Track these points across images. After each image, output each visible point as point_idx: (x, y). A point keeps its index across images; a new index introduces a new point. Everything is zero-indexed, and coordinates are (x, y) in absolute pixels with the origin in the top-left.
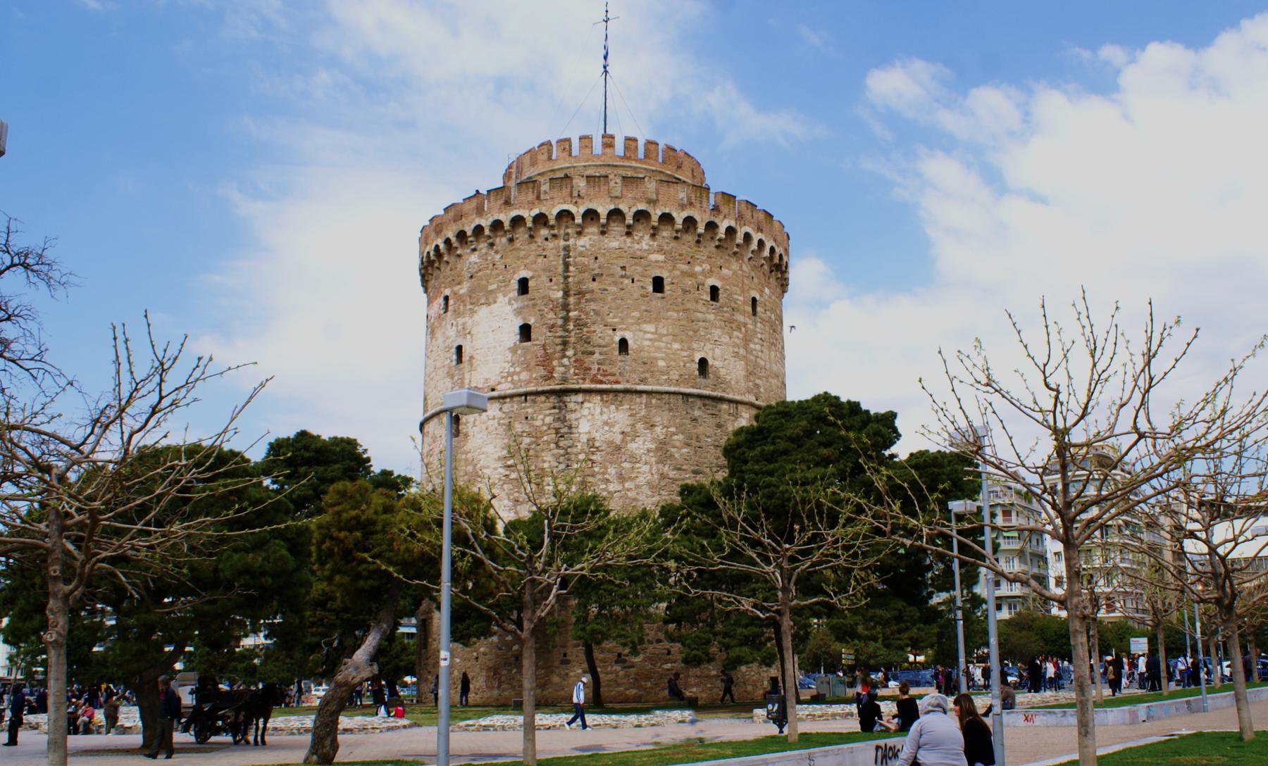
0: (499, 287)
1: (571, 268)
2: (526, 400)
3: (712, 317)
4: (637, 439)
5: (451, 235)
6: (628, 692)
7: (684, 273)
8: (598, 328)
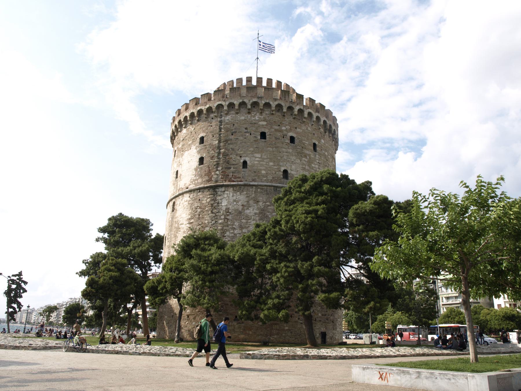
0: (193, 142)
1: (223, 130)
3: (291, 151)
4: (250, 208)
6: (239, 336)
7: (276, 130)
8: (233, 156)
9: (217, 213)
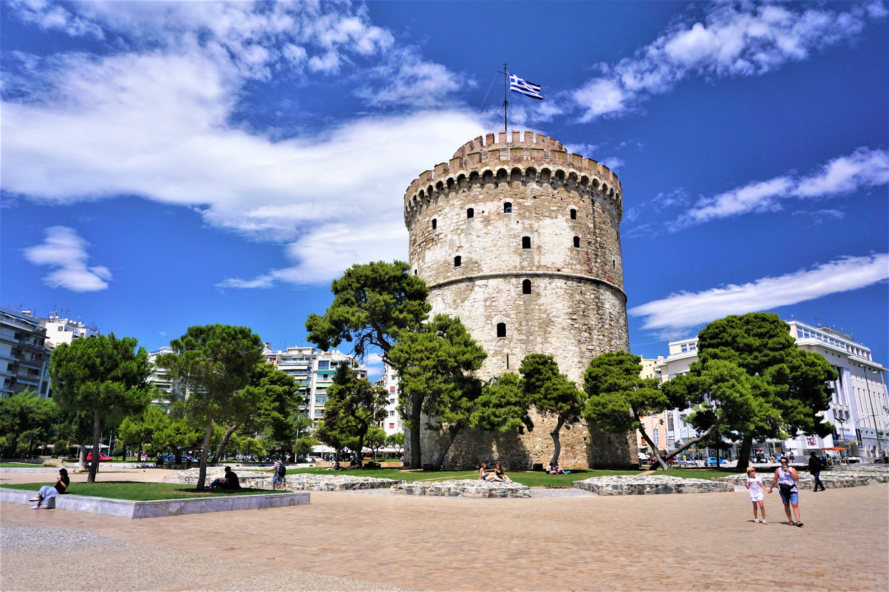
0: (558, 210)
5: (520, 166)
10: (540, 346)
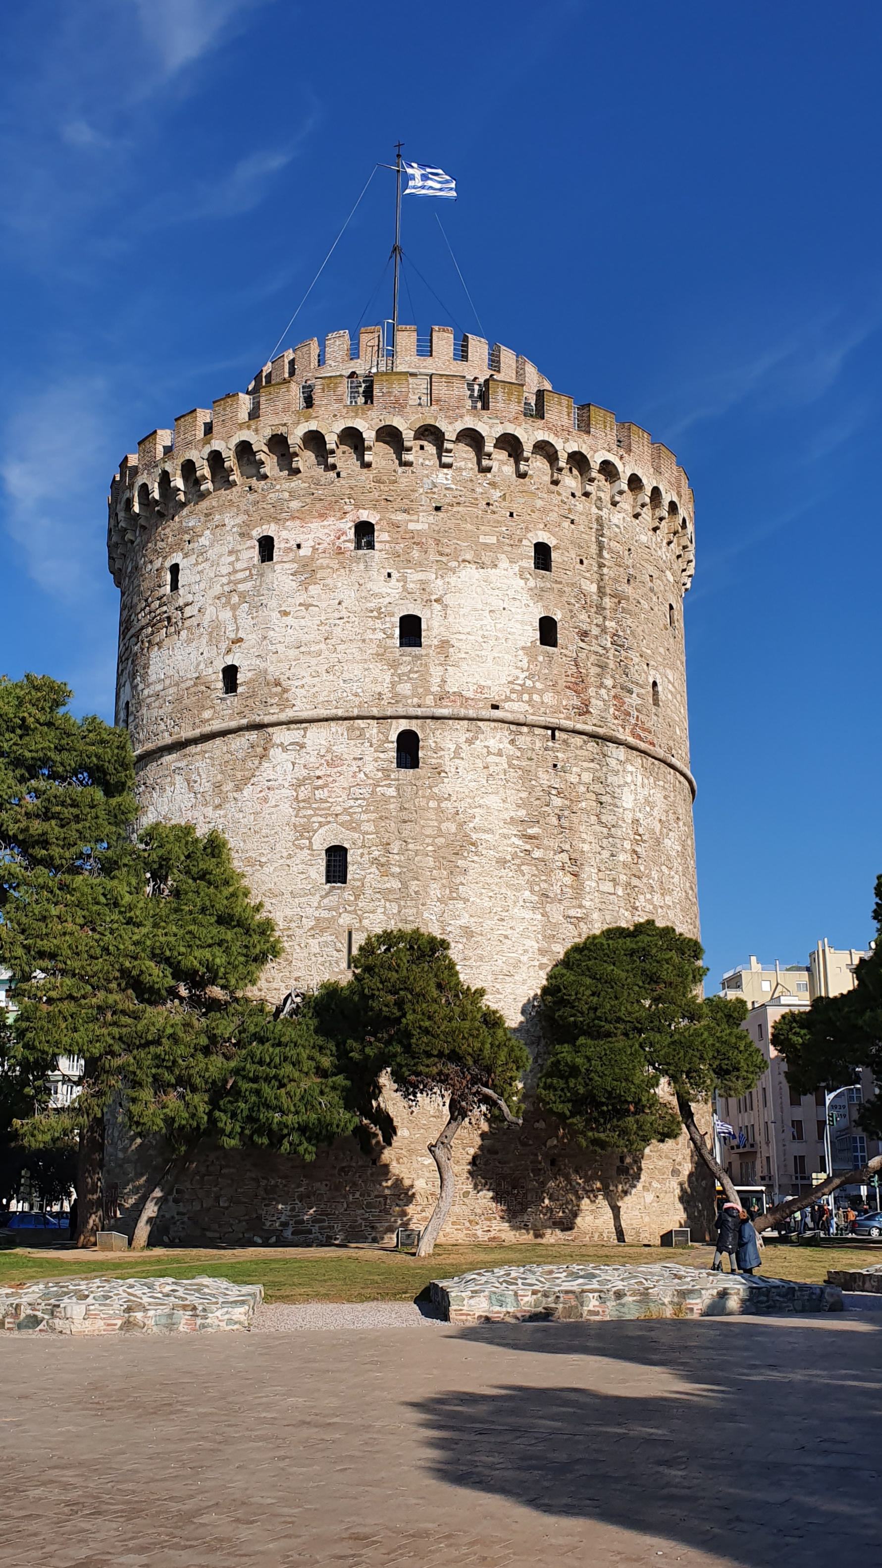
1: (605, 553)
2: (553, 737)
9: (613, 826)
10: (438, 908)
